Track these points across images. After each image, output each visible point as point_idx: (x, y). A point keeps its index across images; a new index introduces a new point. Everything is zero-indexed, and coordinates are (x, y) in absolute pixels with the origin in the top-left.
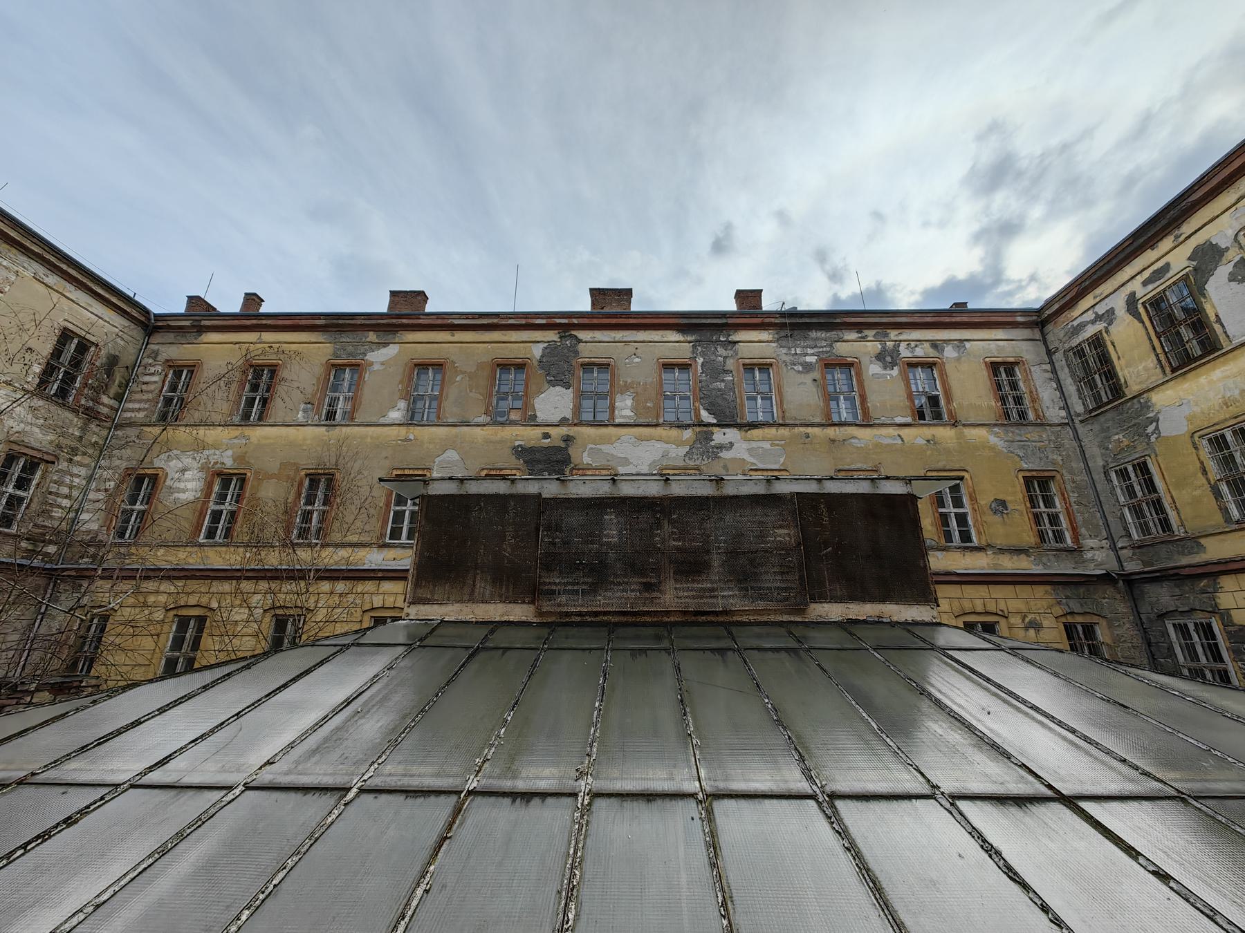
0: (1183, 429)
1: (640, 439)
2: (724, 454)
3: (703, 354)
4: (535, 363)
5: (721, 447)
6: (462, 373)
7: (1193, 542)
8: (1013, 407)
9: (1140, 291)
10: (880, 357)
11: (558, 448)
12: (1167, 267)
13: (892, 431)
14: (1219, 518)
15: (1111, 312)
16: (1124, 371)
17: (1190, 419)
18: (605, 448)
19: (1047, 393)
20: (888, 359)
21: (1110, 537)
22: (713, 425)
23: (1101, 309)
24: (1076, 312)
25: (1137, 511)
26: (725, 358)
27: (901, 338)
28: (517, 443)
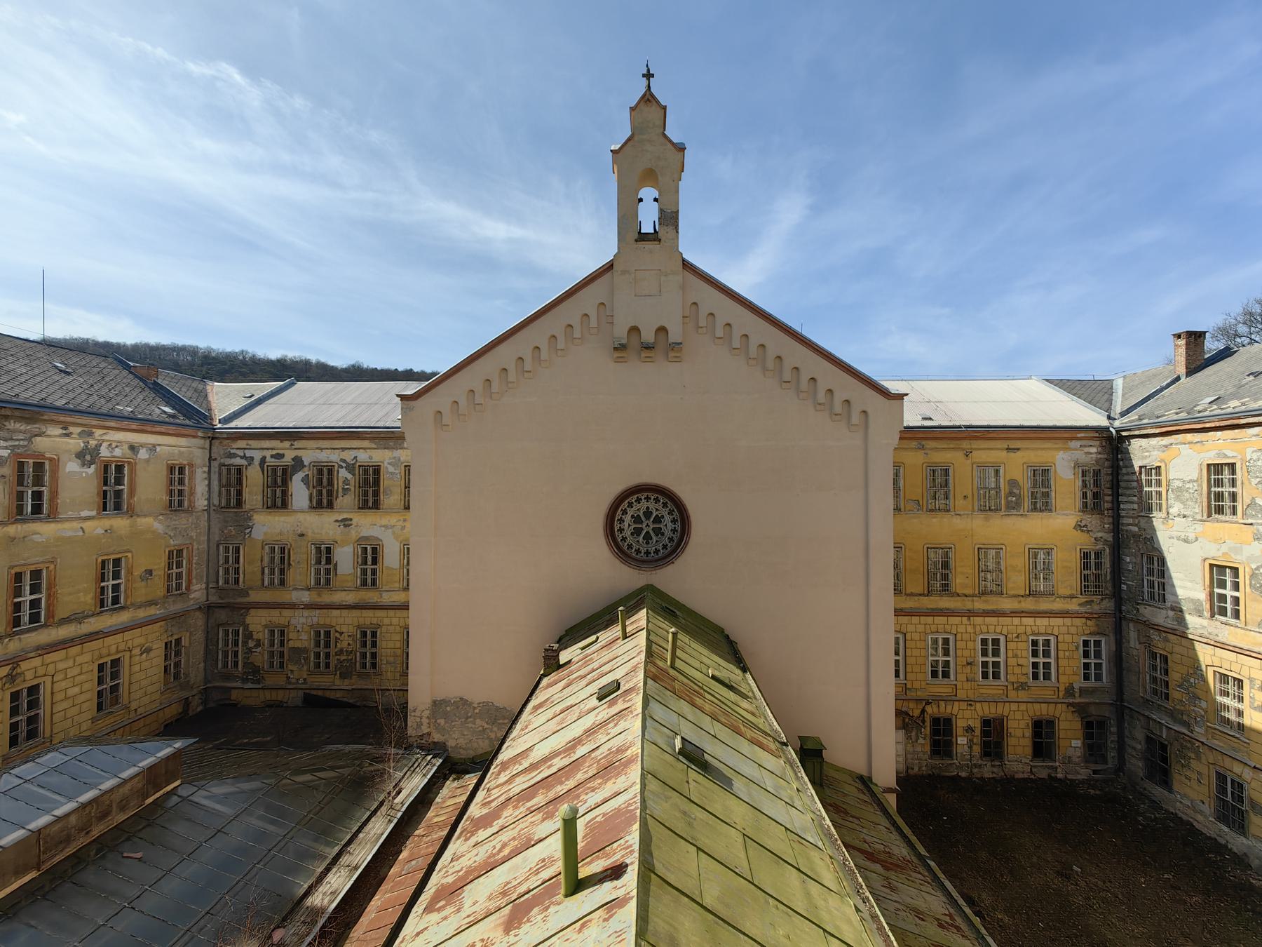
0: (261, 538)
7: (245, 593)
8: (177, 500)
9: (268, 459)
10: (80, 455)
12: (282, 456)
13: (75, 525)
14: (259, 583)
15: (252, 458)
17: (265, 534)
20: (88, 457)
21: (207, 584)
23: (248, 453)
24: (235, 446)
25: (227, 571)
27: (105, 437)
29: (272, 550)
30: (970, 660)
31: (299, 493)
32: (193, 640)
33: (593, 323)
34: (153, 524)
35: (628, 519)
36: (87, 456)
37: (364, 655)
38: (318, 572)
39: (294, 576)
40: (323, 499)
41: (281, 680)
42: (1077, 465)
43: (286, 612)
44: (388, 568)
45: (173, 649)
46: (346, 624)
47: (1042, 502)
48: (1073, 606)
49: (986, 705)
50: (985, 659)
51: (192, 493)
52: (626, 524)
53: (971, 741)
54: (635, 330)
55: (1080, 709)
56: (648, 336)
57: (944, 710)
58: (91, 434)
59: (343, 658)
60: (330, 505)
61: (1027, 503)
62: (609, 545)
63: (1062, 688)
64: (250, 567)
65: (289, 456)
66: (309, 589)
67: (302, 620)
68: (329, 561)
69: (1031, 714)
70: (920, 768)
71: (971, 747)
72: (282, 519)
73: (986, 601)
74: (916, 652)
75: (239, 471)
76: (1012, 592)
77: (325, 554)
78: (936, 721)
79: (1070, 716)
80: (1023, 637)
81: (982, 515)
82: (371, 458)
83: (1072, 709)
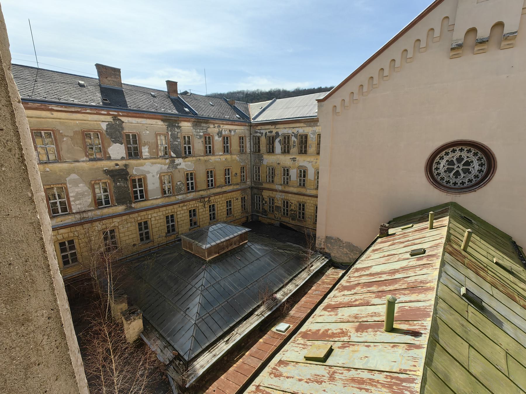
1: (153, 163)
2: (179, 167)
3: (171, 131)
4: (104, 132)
5: (177, 165)
6: (67, 136)
9: (268, 133)
11: (123, 170)
13: (219, 157)
16: (261, 148)
18: (141, 168)
19: (248, 145)
22: (175, 157)
23: (261, 131)
25: (256, 175)
26: (178, 132)
28: (105, 169)
29: (269, 169)
31: (278, 147)
32: (248, 198)
33: (437, 33)
34: (236, 157)
35: (443, 163)
36: (220, 134)
37: (300, 213)
38: (284, 178)
39: (276, 179)
40: (286, 151)
41: (273, 217)
43: (274, 193)
44: (310, 180)
45: (243, 199)
46: (294, 200)
51: (246, 147)
52: (442, 165)
54: (473, 30)
56: (483, 32)
58: (220, 126)
59: (292, 212)
60: (288, 152)
62: (428, 177)
64: (263, 175)
65: (274, 131)
66: (281, 185)
67: (279, 196)
68: (288, 175)
72: (272, 157)
75: (259, 138)
77: (286, 172)
82: (304, 131)
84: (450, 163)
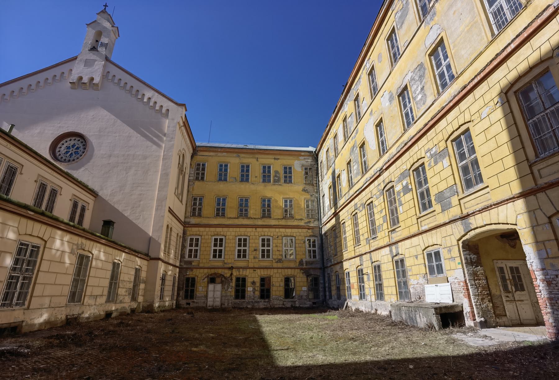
30: (256, 248)
35: (63, 147)
42: (303, 166)
47: (288, 179)
48: (302, 223)
49: (262, 270)
50: (263, 248)
53: (254, 289)
55: (307, 272)
57: (243, 273)
61: (282, 180)
63: (298, 261)
69: (284, 274)
70: (228, 304)
71: (254, 293)
73: (264, 221)
74: (230, 245)
76: (276, 217)
78: (238, 279)
79: (301, 275)
80: (280, 238)
81: (263, 184)
83: (302, 271)
84: (68, 148)
